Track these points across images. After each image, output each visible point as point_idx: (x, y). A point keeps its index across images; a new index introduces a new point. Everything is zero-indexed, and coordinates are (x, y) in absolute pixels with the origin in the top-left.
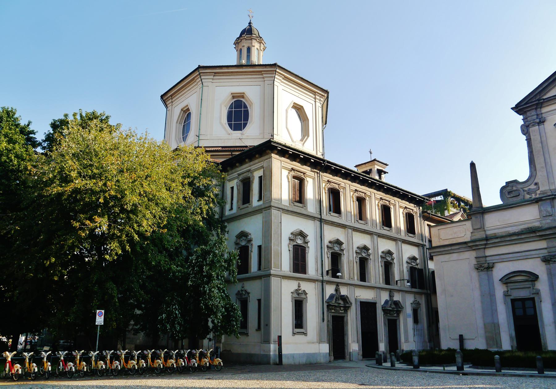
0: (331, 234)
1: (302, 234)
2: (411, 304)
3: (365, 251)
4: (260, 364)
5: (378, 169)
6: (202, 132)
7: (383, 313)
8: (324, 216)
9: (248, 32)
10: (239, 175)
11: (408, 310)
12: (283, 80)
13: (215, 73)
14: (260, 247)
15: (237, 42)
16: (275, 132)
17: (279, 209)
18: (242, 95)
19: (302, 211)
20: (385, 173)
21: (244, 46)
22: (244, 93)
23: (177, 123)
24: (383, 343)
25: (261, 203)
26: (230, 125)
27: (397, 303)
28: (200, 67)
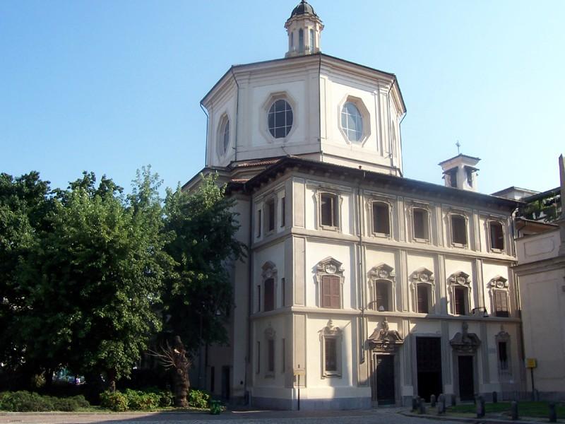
0: (374, 259)
1: (334, 263)
2: (496, 336)
3: (426, 276)
4: (277, 409)
5: (465, 167)
6: (240, 143)
7: (451, 349)
8: (366, 238)
9: (300, 11)
10: (265, 196)
11: (492, 344)
12: (332, 71)
13: (251, 72)
14: (283, 279)
15: (288, 25)
16: (323, 135)
17: (302, 235)
18: (284, 94)
19: (335, 235)
20: (476, 170)
21: (295, 29)
22: (284, 92)
23: (218, 131)
24: (450, 384)
25: (283, 229)
26: (272, 131)
27: (473, 337)
28: (233, 67)
